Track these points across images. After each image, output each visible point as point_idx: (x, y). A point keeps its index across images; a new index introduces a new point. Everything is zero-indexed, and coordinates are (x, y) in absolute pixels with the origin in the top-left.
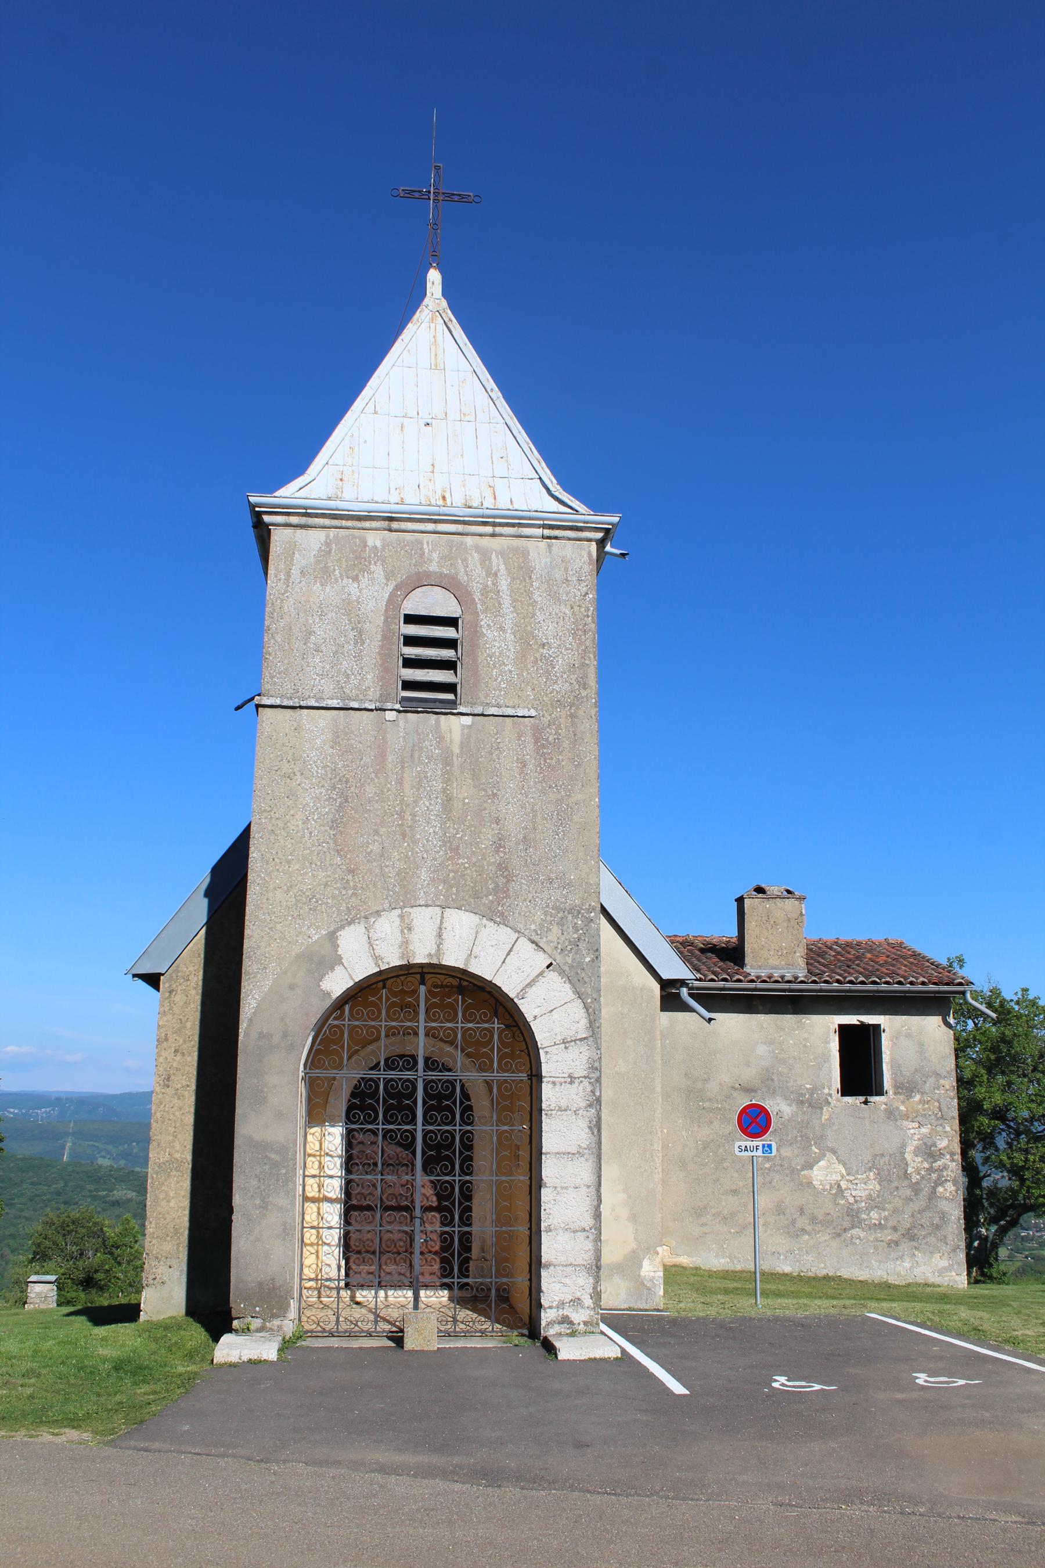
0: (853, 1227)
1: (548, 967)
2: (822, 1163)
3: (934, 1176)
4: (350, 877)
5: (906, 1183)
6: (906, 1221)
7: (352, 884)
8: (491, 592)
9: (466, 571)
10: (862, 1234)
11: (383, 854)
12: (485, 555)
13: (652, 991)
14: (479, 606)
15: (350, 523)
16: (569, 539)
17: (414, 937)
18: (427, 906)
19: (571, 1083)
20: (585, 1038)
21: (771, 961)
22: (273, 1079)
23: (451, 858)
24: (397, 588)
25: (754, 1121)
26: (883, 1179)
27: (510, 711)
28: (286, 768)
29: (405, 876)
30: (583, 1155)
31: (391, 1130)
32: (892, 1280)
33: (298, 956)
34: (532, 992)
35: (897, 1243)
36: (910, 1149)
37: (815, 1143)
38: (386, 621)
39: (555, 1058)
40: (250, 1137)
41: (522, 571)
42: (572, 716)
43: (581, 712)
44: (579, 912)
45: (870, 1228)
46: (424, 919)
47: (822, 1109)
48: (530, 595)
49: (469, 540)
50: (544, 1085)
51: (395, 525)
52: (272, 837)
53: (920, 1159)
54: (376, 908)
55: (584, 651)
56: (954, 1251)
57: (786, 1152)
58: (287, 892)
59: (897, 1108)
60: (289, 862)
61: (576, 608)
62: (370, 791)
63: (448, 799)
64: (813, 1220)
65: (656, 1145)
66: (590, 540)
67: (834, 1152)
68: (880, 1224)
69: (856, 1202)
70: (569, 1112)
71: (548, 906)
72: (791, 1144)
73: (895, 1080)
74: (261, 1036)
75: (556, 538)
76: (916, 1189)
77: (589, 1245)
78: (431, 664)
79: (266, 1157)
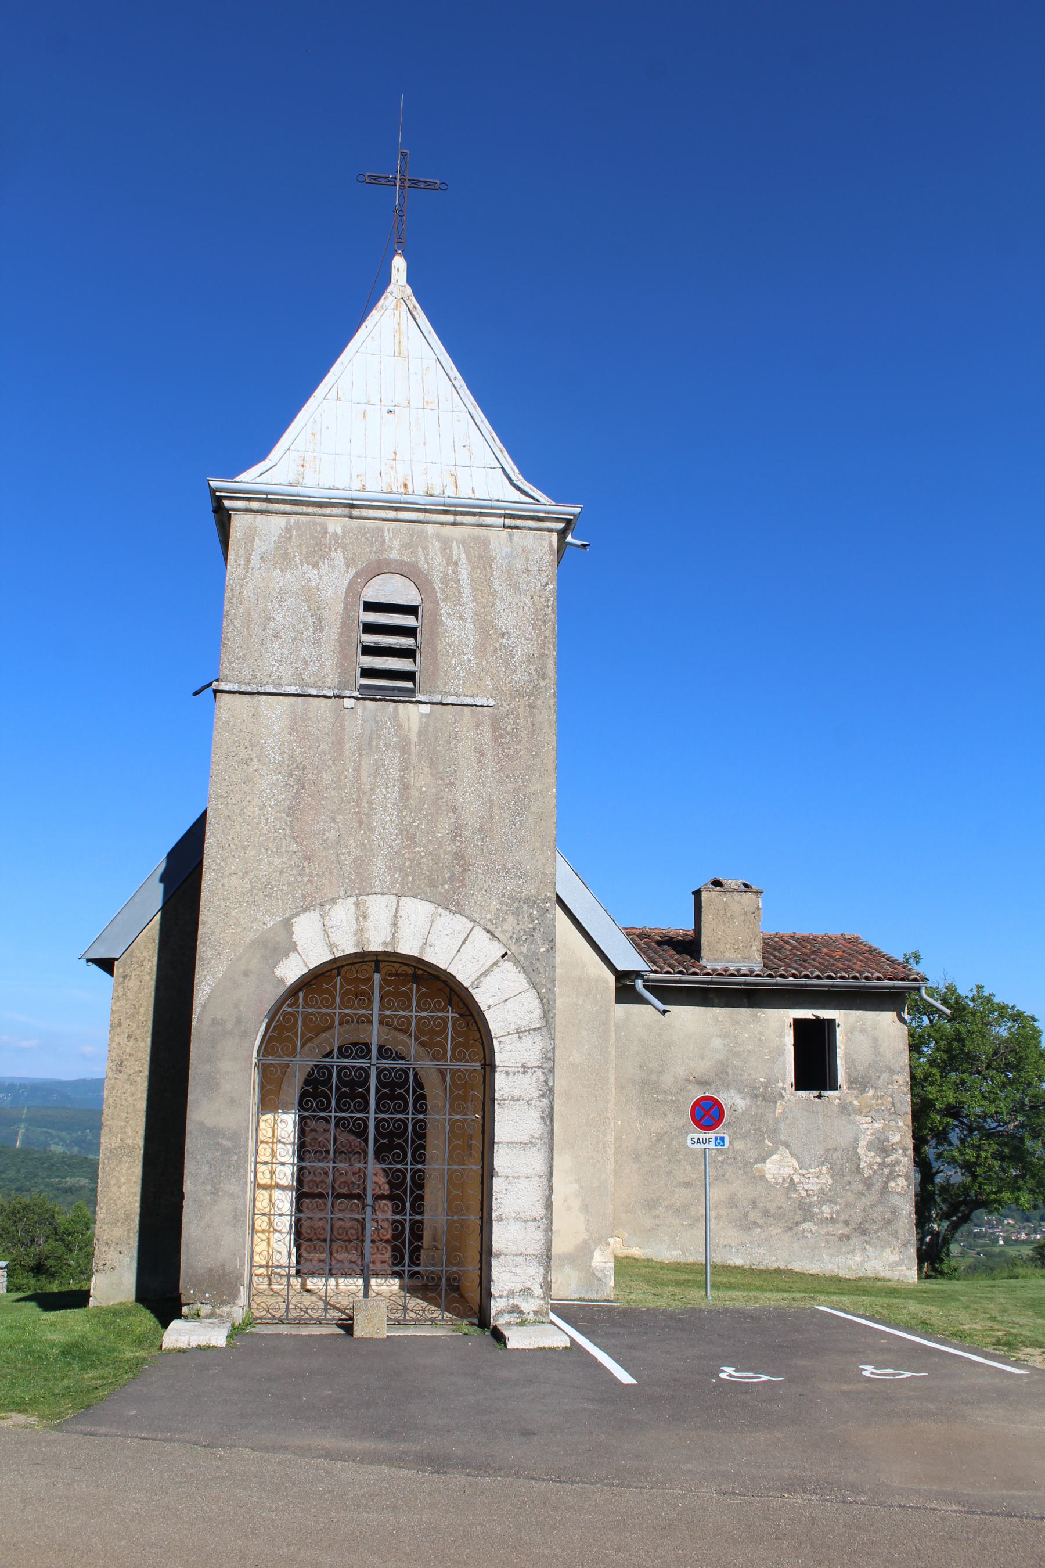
0: (805, 1221)
1: (503, 957)
2: (775, 1157)
3: (886, 1171)
4: (306, 864)
5: (858, 1177)
6: (858, 1214)
7: (307, 871)
8: (451, 580)
9: (426, 560)
10: (814, 1228)
11: (340, 841)
12: (446, 544)
13: (607, 982)
14: (439, 595)
15: (310, 510)
16: (530, 529)
17: (369, 924)
18: (382, 894)
19: (524, 1073)
20: (539, 1028)
21: (727, 955)
22: (226, 1065)
23: (407, 847)
24: (357, 575)
25: (707, 1113)
27: (468, 701)
28: (243, 754)
29: (361, 864)
30: (535, 1146)
31: (344, 1118)
32: (843, 1274)
33: (253, 943)
34: (486, 982)
35: (848, 1238)
36: (862, 1143)
37: (769, 1137)
38: (345, 608)
39: (509, 1047)
40: (202, 1123)
41: (483, 561)
42: (531, 706)
43: (539, 703)
44: (535, 903)
45: (822, 1222)
46: (380, 907)
47: (775, 1102)
48: (490, 584)
49: (430, 528)
50: (497, 1074)
51: (356, 512)
52: (228, 823)
53: (872, 1154)
54: (331, 896)
55: (543, 641)
56: (905, 1245)
57: (739, 1145)
58: (243, 878)
59: (851, 1103)
60: (245, 848)
61: (536, 599)
62: (327, 778)
63: (406, 787)
64: (766, 1213)
65: (608, 1136)
66: (551, 530)
67: (787, 1145)
68: (832, 1218)
69: (808, 1195)
70: (521, 1102)
71: (503, 896)
72: (744, 1138)
74: (215, 1022)
75: (517, 528)
76: (868, 1183)
77: (540, 1235)
78: (390, 651)
79: (218, 1143)
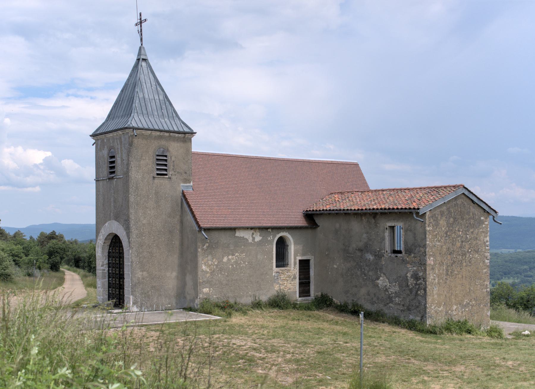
3: (417, 287)
10: (393, 306)
26: (400, 286)
35: (404, 311)
53: (412, 280)
57: (370, 273)
64: (378, 299)
73: (405, 248)
76: (411, 290)
